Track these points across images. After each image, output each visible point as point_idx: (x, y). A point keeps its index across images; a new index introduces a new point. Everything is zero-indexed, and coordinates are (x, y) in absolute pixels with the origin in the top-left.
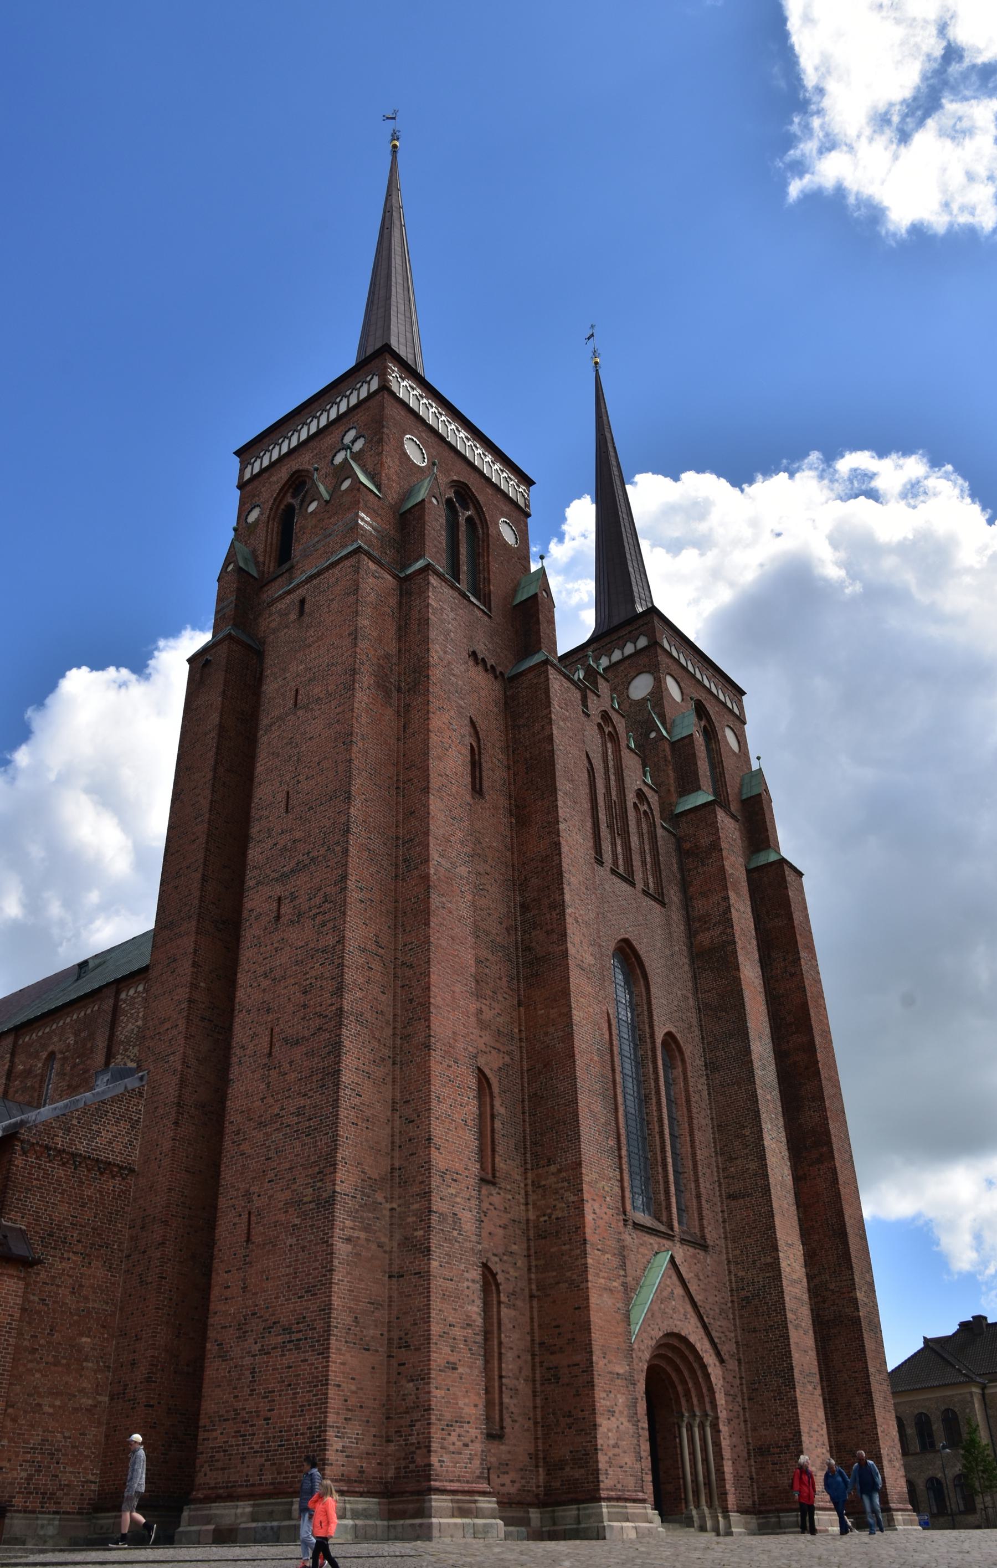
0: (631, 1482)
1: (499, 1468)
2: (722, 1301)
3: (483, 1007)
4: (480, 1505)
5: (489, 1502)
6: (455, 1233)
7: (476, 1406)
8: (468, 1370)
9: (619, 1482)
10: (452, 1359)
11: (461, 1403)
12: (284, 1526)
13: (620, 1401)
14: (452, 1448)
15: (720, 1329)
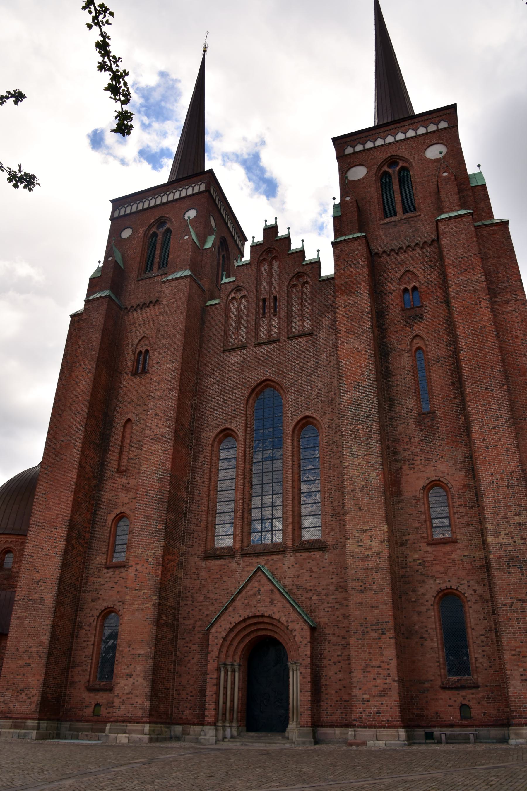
0: (139, 713)
1: (107, 705)
2: (340, 580)
3: (130, 481)
4: (27, 724)
5: (33, 723)
6: (40, 606)
7: (38, 680)
8: (36, 665)
9: (128, 713)
10: (28, 662)
11: (30, 680)
12: (7, 729)
13: (138, 669)
14: (21, 700)
15: (336, 601)
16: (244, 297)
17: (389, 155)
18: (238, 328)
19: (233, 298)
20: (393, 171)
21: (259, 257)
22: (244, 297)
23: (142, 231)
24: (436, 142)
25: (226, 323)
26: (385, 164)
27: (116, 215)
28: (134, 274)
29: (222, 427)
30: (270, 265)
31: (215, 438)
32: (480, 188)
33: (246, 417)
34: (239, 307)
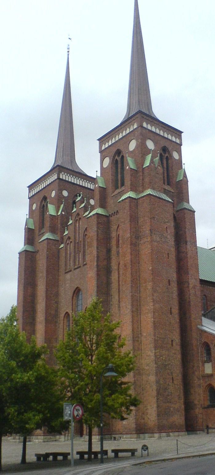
16: (71, 242)
17: (116, 149)
18: (70, 261)
19: (68, 243)
20: (119, 159)
21: (75, 219)
22: (71, 242)
23: (39, 204)
24: (132, 138)
25: (66, 257)
26: (116, 155)
27: (30, 196)
28: (37, 232)
29: (66, 312)
30: (79, 223)
31: (64, 316)
32: (147, 168)
33: (73, 306)
34: (70, 248)
